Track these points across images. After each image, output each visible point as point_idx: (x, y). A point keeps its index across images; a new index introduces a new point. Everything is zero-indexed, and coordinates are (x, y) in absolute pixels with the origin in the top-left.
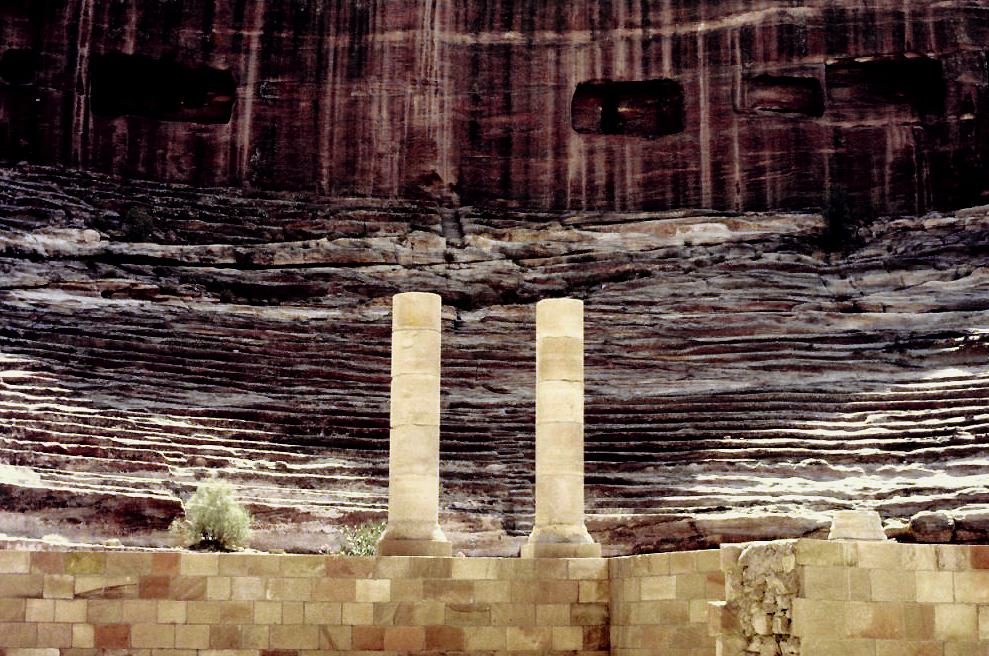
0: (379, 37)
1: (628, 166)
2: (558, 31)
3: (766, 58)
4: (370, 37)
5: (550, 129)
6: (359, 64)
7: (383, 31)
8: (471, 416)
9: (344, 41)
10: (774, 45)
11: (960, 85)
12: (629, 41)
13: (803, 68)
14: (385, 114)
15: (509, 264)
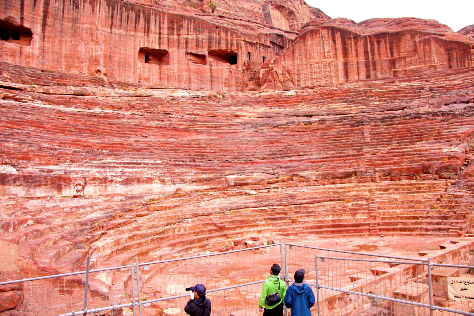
0: (81, 25)
1: (154, 74)
2: (135, 32)
3: (192, 48)
4: (79, 25)
5: (132, 60)
6: (75, 33)
7: (83, 24)
8: (142, 145)
9: (70, 25)
10: (195, 44)
11: (242, 59)
12: (155, 37)
13: (202, 52)
14: (83, 50)
15: (129, 98)
